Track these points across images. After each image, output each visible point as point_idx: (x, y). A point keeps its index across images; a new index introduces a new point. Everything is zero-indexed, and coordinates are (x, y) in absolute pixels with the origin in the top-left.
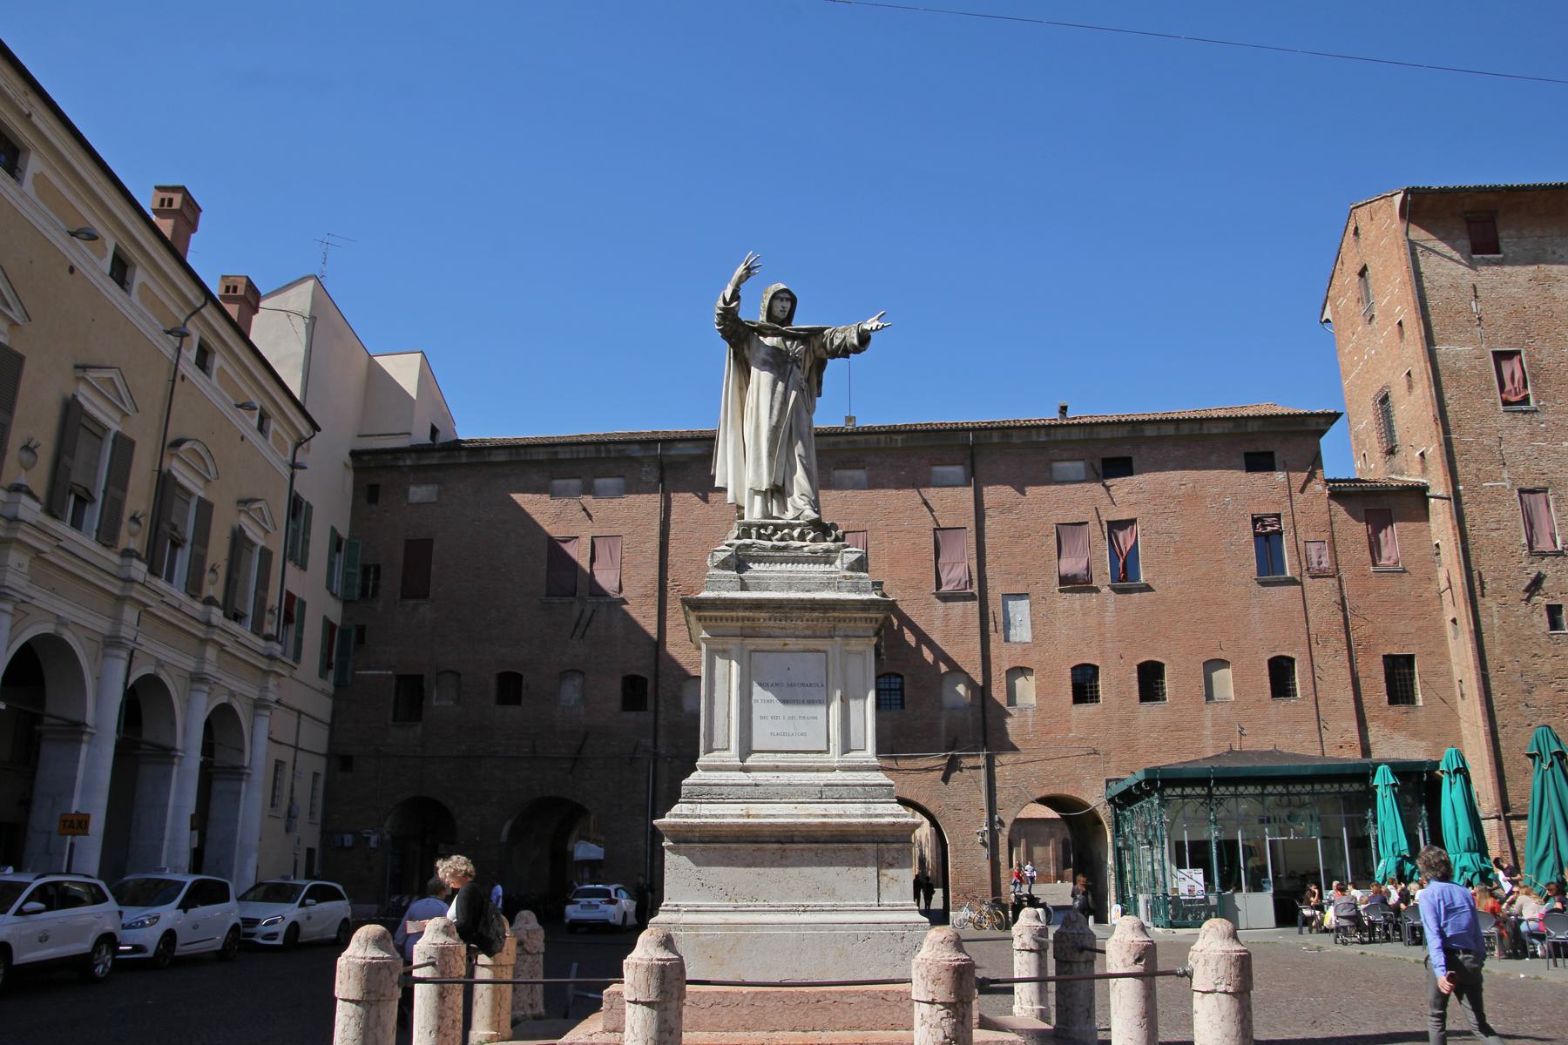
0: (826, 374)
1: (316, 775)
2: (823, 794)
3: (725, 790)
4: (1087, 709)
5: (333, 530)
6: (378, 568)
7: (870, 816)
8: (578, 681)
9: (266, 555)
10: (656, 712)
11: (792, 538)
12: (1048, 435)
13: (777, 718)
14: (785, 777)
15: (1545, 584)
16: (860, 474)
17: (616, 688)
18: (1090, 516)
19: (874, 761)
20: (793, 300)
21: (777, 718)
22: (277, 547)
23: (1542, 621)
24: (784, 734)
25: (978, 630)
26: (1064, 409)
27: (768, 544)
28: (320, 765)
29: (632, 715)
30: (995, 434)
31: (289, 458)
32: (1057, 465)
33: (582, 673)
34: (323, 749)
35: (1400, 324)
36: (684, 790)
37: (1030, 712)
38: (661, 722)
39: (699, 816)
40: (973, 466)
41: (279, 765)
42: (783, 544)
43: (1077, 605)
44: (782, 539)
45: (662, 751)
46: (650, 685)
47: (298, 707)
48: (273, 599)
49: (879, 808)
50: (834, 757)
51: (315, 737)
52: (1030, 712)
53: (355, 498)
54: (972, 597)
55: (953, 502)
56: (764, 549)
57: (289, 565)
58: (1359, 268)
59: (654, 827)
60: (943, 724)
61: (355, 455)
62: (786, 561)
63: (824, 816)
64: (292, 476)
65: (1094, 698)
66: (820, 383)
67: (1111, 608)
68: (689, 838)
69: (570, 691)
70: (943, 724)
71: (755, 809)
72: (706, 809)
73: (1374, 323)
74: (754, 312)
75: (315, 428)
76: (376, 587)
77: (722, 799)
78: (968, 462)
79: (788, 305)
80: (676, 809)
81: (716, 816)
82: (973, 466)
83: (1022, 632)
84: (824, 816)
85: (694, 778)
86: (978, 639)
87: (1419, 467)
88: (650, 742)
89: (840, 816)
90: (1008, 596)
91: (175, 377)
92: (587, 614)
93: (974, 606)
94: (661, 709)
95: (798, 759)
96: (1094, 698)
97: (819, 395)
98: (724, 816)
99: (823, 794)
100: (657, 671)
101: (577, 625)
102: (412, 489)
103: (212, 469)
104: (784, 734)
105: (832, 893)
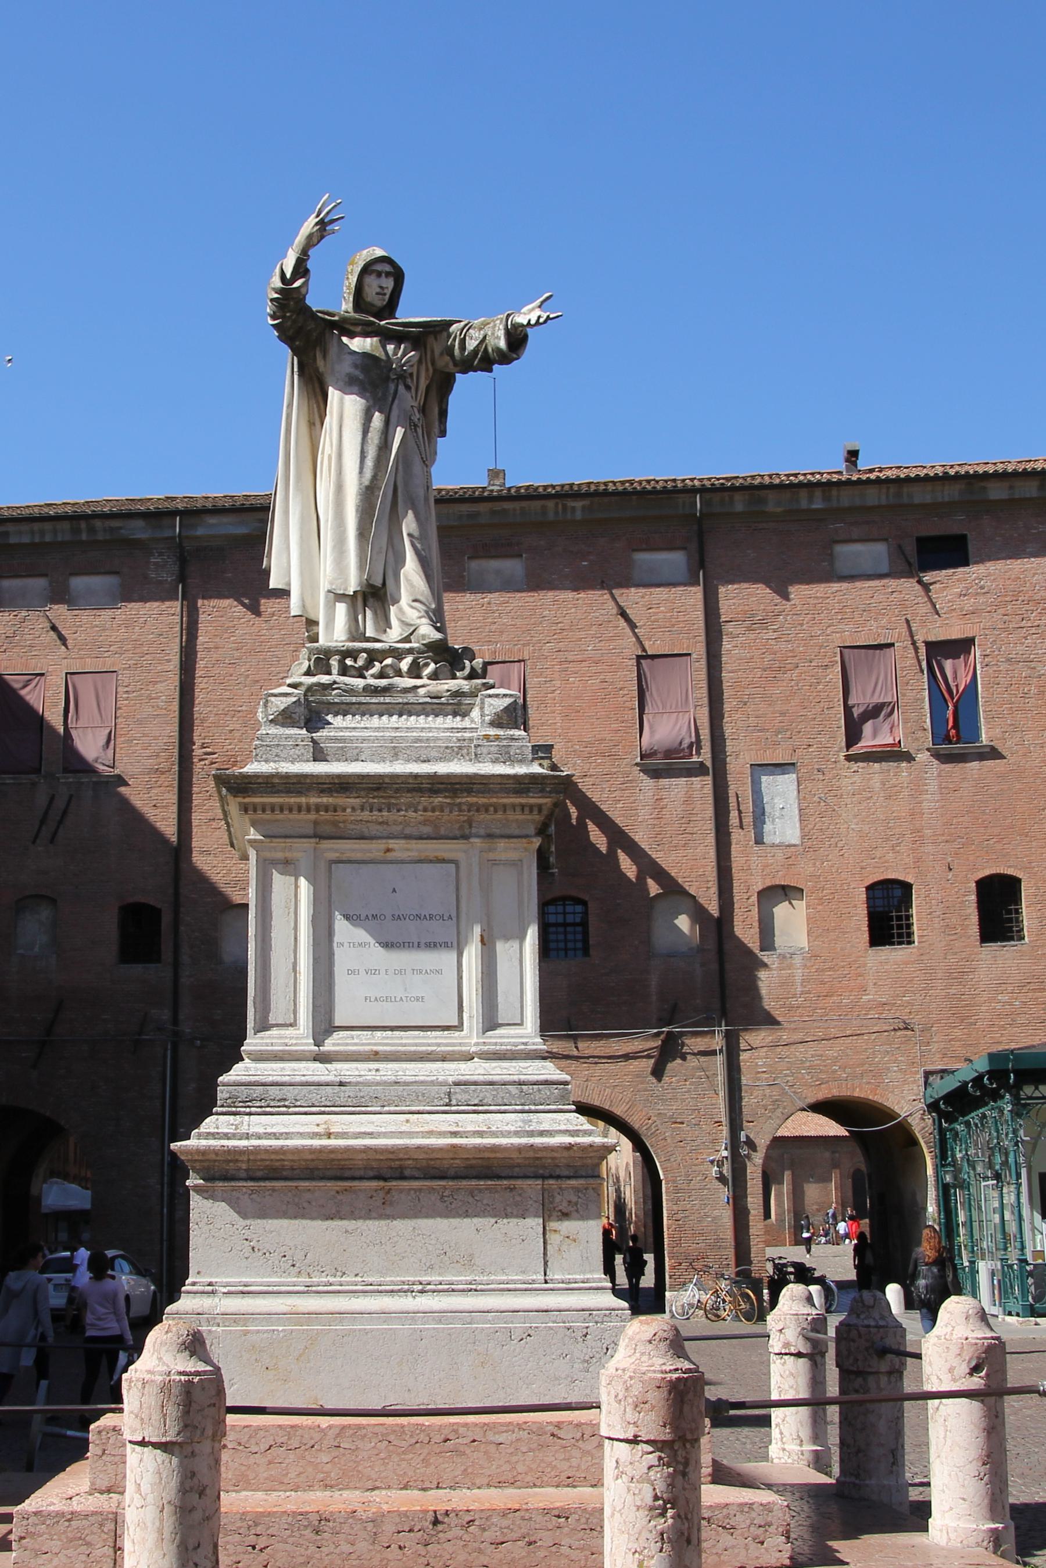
0: (454, 400)
2: (452, 1098)
3: (290, 1092)
4: (892, 955)
7: (531, 1134)
8: (45, 913)
10: (176, 965)
11: (399, 673)
12: (826, 498)
13: (375, 972)
14: (389, 1070)
17: (109, 926)
18: (897, 634)
19: (537, 1043)
20: (398, 276)
21: (375, 972)
24: (388, 999)
25: (710, 825)
26: (853, 455)
27: (360, 683)
29: (137, 970)
30: (737, 496)
32: (841, 549)
33: (53, 901)
36: (222, 1093)
37: (797, 960)
38: (183, 980)
39: (248, 1136)
42: (383, 682)
43: (876, 782)
44: (381, 675)
45: (186, 1029)
46: (166, 919)
49: (546, 1122)
50: (471, 1037)
52: (797, 960)
54: (700, 770)
56: (351, 691)
59: (173, 1155)
60: (654, 981)
63: (455, 1134)
65: (906, 938)
66: (443, 414)
67: (933, 786)
68: (232, 1172)
69: (33, 931)
70: (654, 981)
71: (340, 1123)
72: (257, 1124)
74: (333, 296)
77: (283, 1107)
79: (389, 284)
80: (209, 1124)
81: (275, 1136)
83: (784, 827)
84: (455, 1134)
85: (238, 1072)
86: (711, 839)
88: (166, 1015)
89: (480, 1134)
90: (760, 768)
92: (60, 803)
93: (703, 785)
94: (185, 959)
96: (906, 938)
97: (443, 433)
98: (287, 1135)
99: (452, 1098)
100: (177, 894)
101: (42, 822)
104: (388, 999)
105: (468, 1262)
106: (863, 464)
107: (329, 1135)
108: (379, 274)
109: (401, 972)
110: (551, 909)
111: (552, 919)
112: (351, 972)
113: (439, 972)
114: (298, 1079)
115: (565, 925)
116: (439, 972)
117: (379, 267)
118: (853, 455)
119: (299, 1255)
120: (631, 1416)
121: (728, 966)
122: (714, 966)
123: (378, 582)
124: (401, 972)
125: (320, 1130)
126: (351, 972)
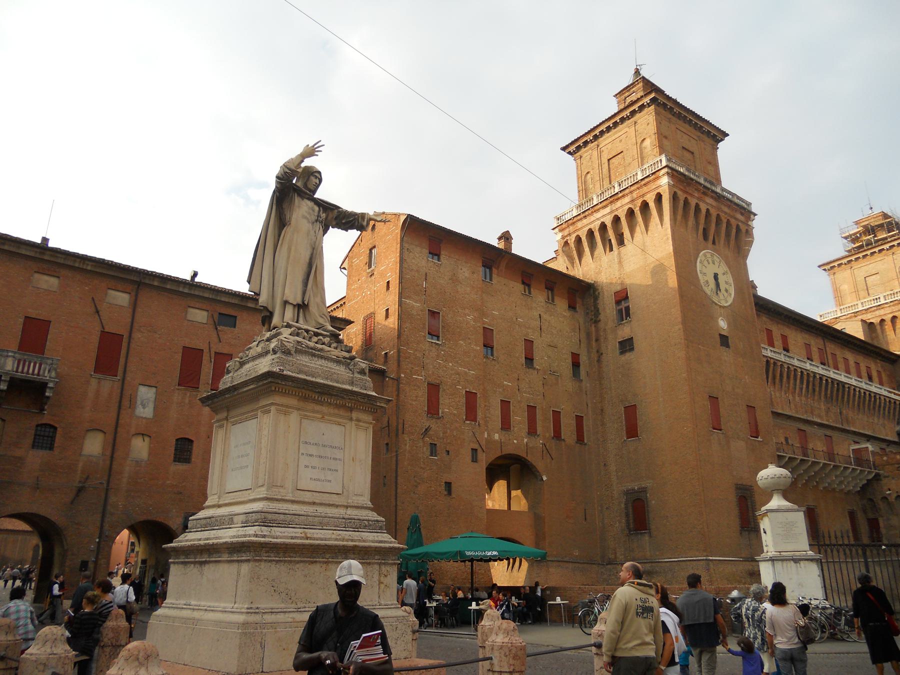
4: (182, 467)
11: (323, 344)
14: (321, 509)
15: (431, 432)
19: (369, 504)
23: (427, 450)
24: (318, 480)
26: (195, 274)
35: (388, 282)
40: (136, 296)
56: (307, 347)
58: (370, 246)
60: (81, 465)
62: (322, 357)
65: (187, 460)
68: (179, 551)
70: (81, 465)
72: (277, 531)
73: (373, 277)
77: (286, 524)
78: (133, 294)
82: (136, 296)
87: (383, 360)
95: (326, 499)
96: (187, 460)
104: (318, 480)
106: (197, 280)
107: (307, 538)
108: (316, 177)
109: (324, 469)
110: (39, 428)
111: (38, 433)
112: (306, 466)
113: (337, 471)
114: (291, 512)
115: (44, 436)
116: (337, 471)
117: (317, 175)
118: (195, 274)
119: (293, 594)
120: (512, 662)
121: (114, 463)
122: (108, 462)
123: (306, 303)
124: (324, 469)
125: (303, 535)
126: (306, 466)
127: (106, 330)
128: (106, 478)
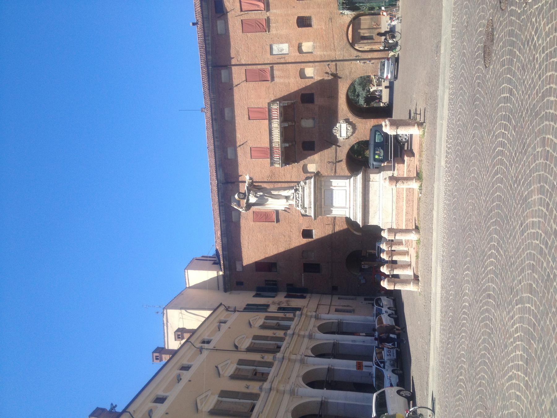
1: (339, 299)
2: (355, 195)
4: (314, 22)
5: (254, 296)
6: (266, 281)
9: (267, 318)
12: (208, 36)
16: (227, 111)
22: (263, 315)
25: (284, 65)
28: (335, 298)
30: (208, 58)
31: (232, 313)
32: (219, 32)
34: (330, 296)
37: (315, 45)
40: (222, 66)
41: (337, 310)
43: (274, 25)
47: (316, 306)
48: (281, 315)
50: (348, 188)
51: (326, 300)
52: (315, 45)
53: (242, 290)
54: (272, 68)
55: (238, 74)
57: (269, 310)
61: (226, 290)
64: (238, 311)
67: (275, 11)
75: (221, 304)
76: (272, 281)
82: (222, 66)
83: (285, 48)
85: (352, 218)
86: (287, 65)
90: (271, 53)
91: (215, 349)
93: (276, 67)
99: (355, 195)
102: (238, 270)
103: (243, 336)
127: (244, 79)
128: (325, 63)
